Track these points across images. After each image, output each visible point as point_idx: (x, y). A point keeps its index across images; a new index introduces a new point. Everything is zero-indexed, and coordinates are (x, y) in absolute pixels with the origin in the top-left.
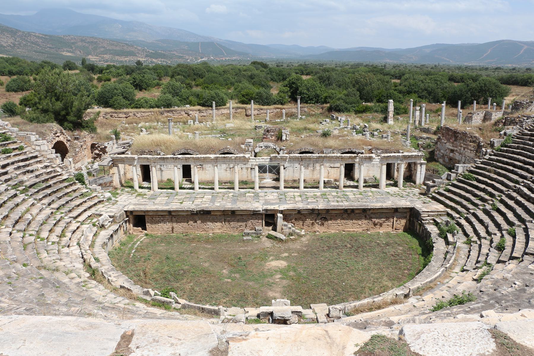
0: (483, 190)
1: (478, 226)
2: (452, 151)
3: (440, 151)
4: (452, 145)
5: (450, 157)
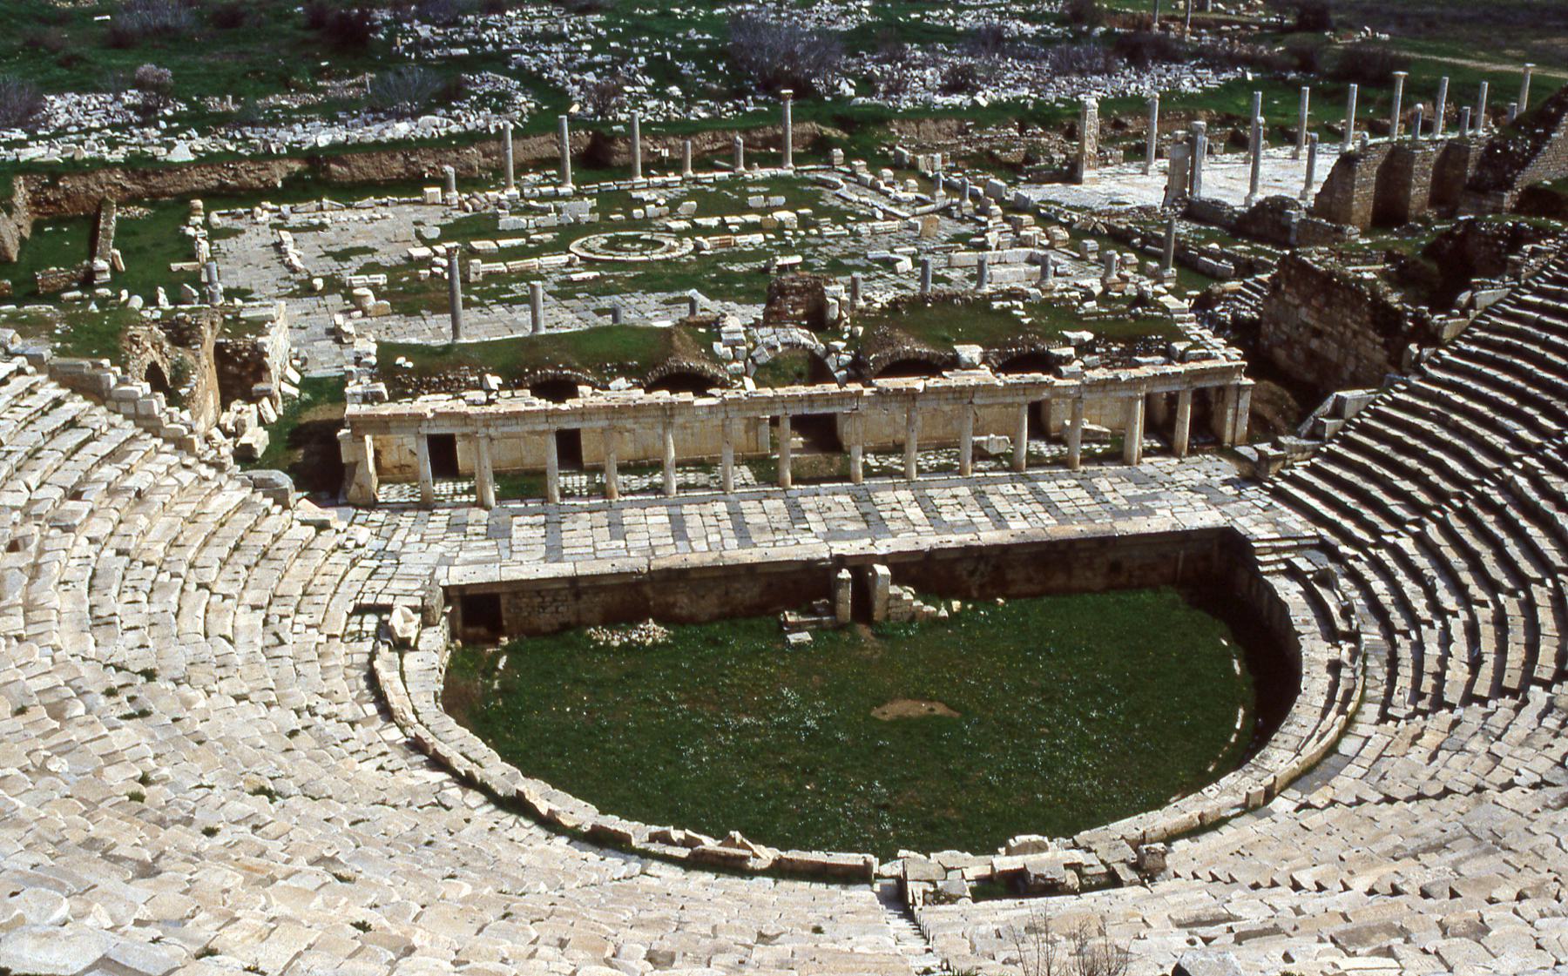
0: (1414, 476)
1: (1409, 586)
2: (1317, 333)
3: (1277, 325)
5: (1311, 349)
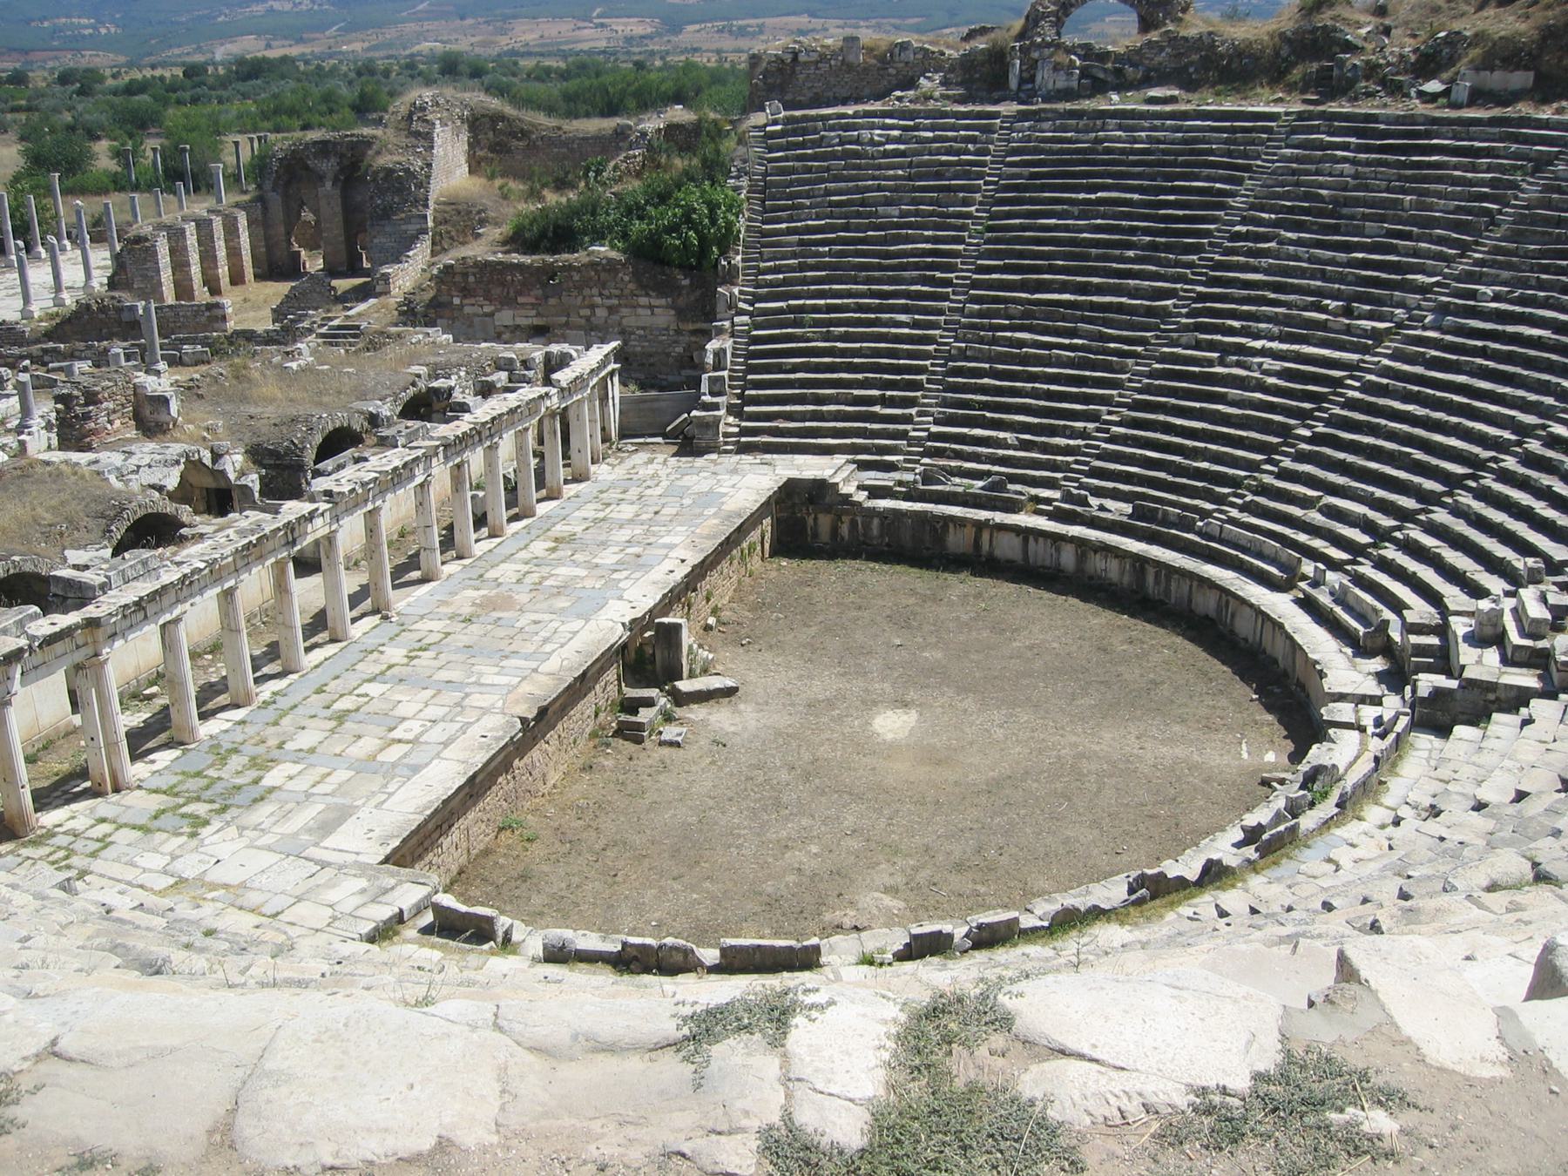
4: (534, 313)
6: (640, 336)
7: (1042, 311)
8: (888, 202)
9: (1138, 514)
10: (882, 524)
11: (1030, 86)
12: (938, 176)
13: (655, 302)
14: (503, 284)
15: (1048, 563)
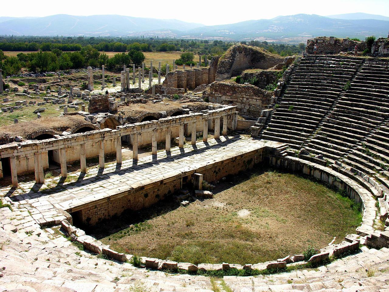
6: (253, 106)
7: (353, 112)
8: (325, 79)
9: (352, 170)
10: (288, 163)
11: (377, 52)
12: (341, 74)
13: (257, 98)
14: (224, 90)
15: (326, 181)
